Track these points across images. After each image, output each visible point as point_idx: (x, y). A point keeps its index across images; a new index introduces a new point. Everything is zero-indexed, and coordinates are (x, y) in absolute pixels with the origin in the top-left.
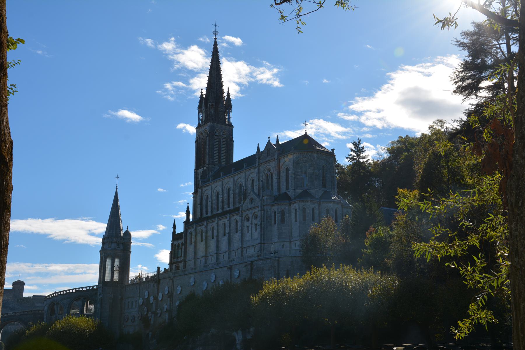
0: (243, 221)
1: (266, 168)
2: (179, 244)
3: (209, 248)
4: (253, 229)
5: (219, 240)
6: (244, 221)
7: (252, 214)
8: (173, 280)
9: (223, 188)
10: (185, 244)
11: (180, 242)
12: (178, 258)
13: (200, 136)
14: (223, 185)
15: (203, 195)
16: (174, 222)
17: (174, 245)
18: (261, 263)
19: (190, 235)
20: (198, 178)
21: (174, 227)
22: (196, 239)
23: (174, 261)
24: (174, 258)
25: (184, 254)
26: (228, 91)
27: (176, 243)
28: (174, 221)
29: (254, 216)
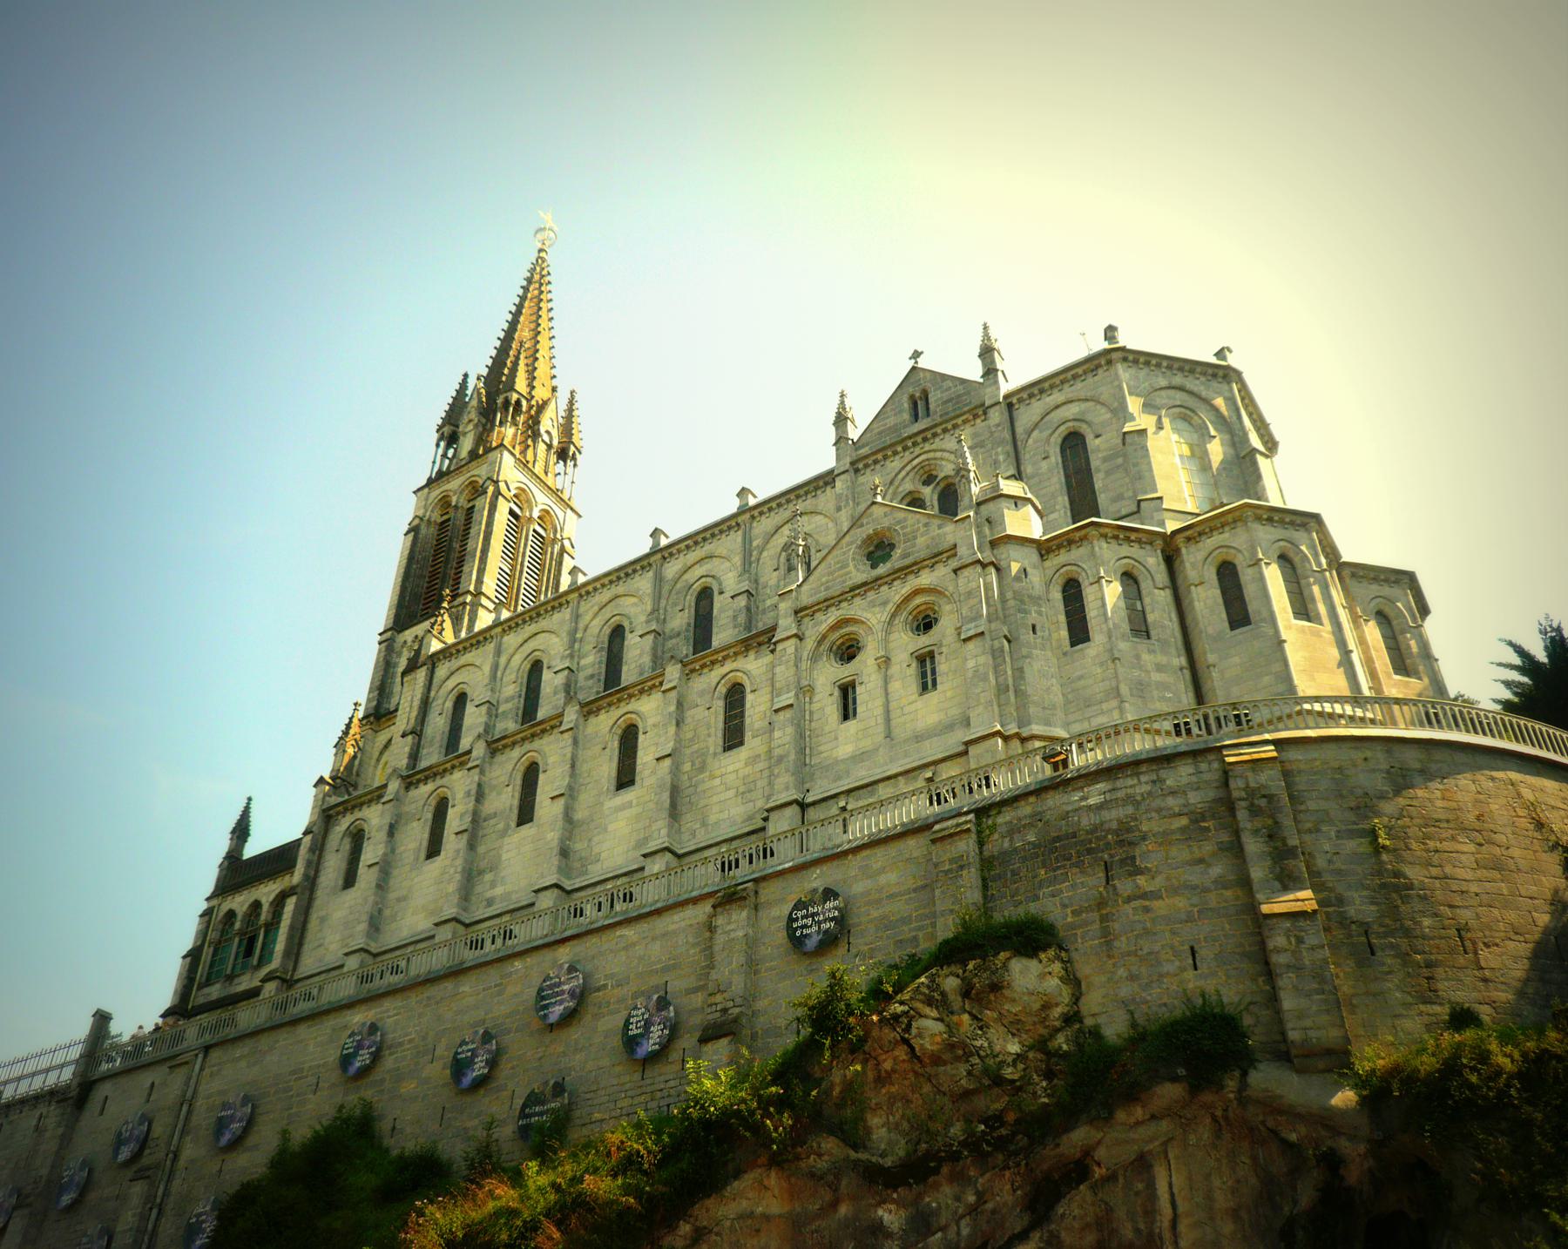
0: (804, 665)
2: (256, 905)
3: (488, 877)
4: (895, 686)
5: (579, 815)
7: (890, 607)
9: (576, 630)
11: (266, 892)
13: (432, 511)
14: (577, 617)
15: (433, 694)
17: (221, 914)
18: (1091, 801)
19: (347, 845)
20: (396, 665)
21: (241, 831)
22: (393, 851)
23: (201, 1000)
24: (208, 983)
25: (290, 938)
26: (571, 402)
27: (239, 903)
28: (248, 804)
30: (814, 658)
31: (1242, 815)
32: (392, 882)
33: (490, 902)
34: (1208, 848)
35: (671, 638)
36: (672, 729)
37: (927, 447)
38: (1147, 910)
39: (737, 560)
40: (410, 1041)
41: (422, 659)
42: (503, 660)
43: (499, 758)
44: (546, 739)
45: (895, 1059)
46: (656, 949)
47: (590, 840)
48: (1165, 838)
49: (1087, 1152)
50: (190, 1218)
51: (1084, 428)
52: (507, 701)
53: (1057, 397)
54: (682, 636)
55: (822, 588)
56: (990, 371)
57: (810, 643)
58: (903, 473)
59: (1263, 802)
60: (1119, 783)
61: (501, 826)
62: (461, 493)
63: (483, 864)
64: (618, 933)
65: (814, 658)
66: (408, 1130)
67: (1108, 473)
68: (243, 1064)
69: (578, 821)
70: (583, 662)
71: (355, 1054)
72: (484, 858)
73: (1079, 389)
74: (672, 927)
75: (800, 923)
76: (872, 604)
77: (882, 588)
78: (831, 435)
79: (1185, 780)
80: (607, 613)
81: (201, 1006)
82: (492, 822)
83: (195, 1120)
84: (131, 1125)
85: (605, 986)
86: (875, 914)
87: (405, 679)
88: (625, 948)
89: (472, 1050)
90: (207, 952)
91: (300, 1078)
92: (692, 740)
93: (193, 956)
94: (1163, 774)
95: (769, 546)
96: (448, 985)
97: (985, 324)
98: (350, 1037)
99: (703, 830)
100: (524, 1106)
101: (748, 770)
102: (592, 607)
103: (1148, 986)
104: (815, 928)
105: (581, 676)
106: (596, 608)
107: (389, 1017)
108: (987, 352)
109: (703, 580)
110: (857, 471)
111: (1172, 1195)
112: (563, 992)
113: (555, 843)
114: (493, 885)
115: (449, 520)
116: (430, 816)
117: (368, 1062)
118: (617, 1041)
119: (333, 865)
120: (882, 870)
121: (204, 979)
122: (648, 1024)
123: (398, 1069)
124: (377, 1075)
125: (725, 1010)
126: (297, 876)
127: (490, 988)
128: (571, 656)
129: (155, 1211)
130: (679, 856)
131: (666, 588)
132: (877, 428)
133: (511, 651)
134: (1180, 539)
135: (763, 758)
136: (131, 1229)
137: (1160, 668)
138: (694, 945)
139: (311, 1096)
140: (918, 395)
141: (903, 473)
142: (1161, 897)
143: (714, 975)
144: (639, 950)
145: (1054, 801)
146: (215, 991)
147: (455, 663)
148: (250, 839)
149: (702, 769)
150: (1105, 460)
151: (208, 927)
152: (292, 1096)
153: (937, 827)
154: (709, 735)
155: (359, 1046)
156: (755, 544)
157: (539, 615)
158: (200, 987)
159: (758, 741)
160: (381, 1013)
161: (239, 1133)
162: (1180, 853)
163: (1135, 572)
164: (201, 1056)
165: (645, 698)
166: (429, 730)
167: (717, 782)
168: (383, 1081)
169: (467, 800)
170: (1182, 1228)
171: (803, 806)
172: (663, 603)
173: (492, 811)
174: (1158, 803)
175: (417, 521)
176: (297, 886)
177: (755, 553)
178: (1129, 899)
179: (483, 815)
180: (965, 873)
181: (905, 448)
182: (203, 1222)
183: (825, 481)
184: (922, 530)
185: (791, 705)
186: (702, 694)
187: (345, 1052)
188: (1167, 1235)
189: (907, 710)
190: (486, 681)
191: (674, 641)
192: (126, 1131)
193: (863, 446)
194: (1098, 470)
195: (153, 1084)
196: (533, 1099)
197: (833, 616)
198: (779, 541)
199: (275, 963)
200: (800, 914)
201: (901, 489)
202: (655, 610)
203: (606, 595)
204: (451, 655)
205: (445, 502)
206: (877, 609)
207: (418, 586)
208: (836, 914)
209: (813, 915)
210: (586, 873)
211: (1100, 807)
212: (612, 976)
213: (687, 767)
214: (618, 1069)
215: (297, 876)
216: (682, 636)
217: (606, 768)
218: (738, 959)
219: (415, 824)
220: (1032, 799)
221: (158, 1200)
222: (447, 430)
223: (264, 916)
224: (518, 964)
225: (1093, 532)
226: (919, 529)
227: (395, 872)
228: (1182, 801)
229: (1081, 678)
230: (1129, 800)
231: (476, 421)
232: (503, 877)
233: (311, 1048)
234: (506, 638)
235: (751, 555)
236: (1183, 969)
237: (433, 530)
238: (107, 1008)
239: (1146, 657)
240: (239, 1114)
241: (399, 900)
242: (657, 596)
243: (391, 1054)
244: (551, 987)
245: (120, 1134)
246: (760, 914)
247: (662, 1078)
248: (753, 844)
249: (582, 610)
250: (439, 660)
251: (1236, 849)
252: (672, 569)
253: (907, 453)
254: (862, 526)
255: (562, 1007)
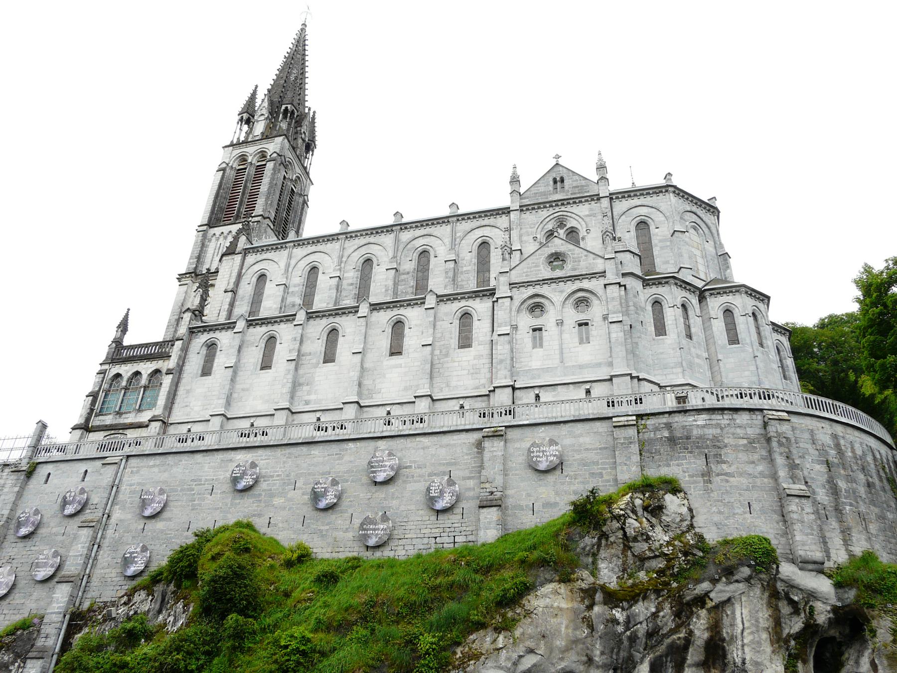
1: (552, 217)
2: (137, 373)
3: (305, 388)
4: (566, 336)
6: (519, 311)
7: (565, 294)
8: (122, 467)
10: (178, 372)
11: (146, 368)
12: (119, 413)
13: (234, 162)
15: (244, 271)
16: (127, 316)
17: (112, 375)
18: (699, 423)
19: (204, 351)
21: (123, 326)
22: (239, 361)
24: (100, 414)
25: (168, 399)
27: (126, 370)
28: (128, 312)
29: (572, 300)
30: (519, 311)
31: (774, 444)
32: (238, 379)
33: (307, 403)
34: (756, 457)
35: (404, 274)
36: (431, 331)
37: (563, 208)
38: (727, 481)
39: (447, 241)
40: (278, 476)
41: (238, 250)
42: (293, 262)
43: (312, 322)
44: (344, 317)
45: (616, 536)
46: (443, 452)
47: (374, 380)
48: (736, 448)
49: (707, 594)
50: (125, 554)
51: (649, 221)
52: (295, 286)
53: (636, 201)
54: (411, 274)
55: (524, 275)
56: (603, 179)
57: (517, 302)
58: (548, 219)
59: (784, 440)
60: (713, 417)
61: (314, 361)
62: (255, 156)
63: (302, 380)
64: (417, 439)
65: (519, 311)
66: (280, 525)
67: (662, 248)
68: (156, 470)
69: (366, 368)
70: (346, 275)
71: (241, 478)
72: (303, 377)
73: (648, 200)
74: (452, 442)
75: (535, 454)
76: (555, 290)
77: (560, 283)
78: (509, 189)
79: (745, 422)
80: (363, 251)
81: (98, 426)
82: (308, 358)
83: (121, 497)
84: (73, 494)
85: (410, 467)
86: (577, 457)
87: (224, 258)
88: (423, 448)
89: (325, 488)
90: (101, 395)
91: (199, 485)
92: (439, 338)
93: (94, 395)
94: (735, 416)
95: (466, 238)
96: (304, 449)
97: (599, 151)
98: (237, 467)
99: (447, 389)
100: (362, 524)
101: (475, 362)
102: (354, 245)
103: (727, 518)
104: (544, 459)
105: (345, 282)
106: (356, 247)
107: (261, 460)
108: (601, 167)
109: (425, 247)
110: (522, 210)
111: (742, 618)
112: (386, 466)
113: (356, 378)
114: (309, 393)
115: (245, 169)
116: (263, 346)
117: (251, 483)
118: (420, 498)
119: (195, 361)
120: (581, 435)
121: (98, 411)
122: (442, 492)
123: (271, 490)
124: (256, 491)
125: (492, 493)
126: (172, 363)
127: (333, 455)
128: (340, 270)
129: (96, 546)
130: (433, 400)
131: (401, 247)
132: (534, 190)
133: (299, 258)
134: (707, 294)
135: (484, 357)
136: (81, 555)
137: (698, 356)
138: (467, 454)
139: (209, 496)
140: (558, 179)
141: (548, 219)
142: (734, 477)
143: (484, 472)
144: (432, 450)
145: (678, 419)
146: (108, 420)
147: (259, 257)
148: (127, 333)
149: (447, 355)
150: (660, 241)
151: (103, 381)
152: (194, 494)
153: (614, 419)
154: (451, 338)
155: (244, 473)
156: (458, 235)
157: (318, 242)
158: (96, 416)
159: (481, 347)
160: (256, 456)
161: (159, 510)
162: (743, 456)
163: (687, 305)
164: (124, 461)
165: (409, 308)
166: (241, 292)
167: (456, 364)
168: (260, 495)
169: (295, 342)
170: (745, 634)
171: (514, 389)
172: (399, 254)
173: (308, 351)
174: (732, 430)
175: (224, 165)
176: (173, 369)
177: (458, 240)
178: (718, 475)
179: (302, 352)
180: (632, 446)
181: (551, 206)
182: (135, 557)
183: (506, 211)
184: (584, 258)
185: (508, 334)
186: (446, 314)
187: (234, 475)
188: (739, 636)
189: (572, 350)
190: (283, 271)
191: (405, 276)
192: (70, 496)
193: (525, 198)
194: (656, 245)
195: (86, 471)
196: (367, 521)
197: (531, 291)
198: (472, 237)
199: (158, 411)
200: (535, 449)
201: (546, 227)
202: (394, 257)
203: (363, 241)
204: (258, 251)
205: (243, 159)
206: (557, 294)
207: (222, 203)
208: (557, 453)
209: (543, 451)
210: (372, 398)
211: (704, 426)
212: (415, 462)
213: (437, 352)
214: (421, 512)
215: (172, 363)
216: (411, 274)
217: (384, 342)
218: (499, 467)
219: (254, 348)
220: (667, 415)
221: (98, 540)
222: (245, 116)
223: (144, 380)
224: (351, 445)
225: (672, 281)
226: (582, 257)
227: (240, 373)
228: (744, 432)
229: (662, 353)
230: (718, 426)
231: (266, 116)
232: (316, 390)
233: (206, 469)
234: (295, 250)
235: (455, 240)
236: (745, 513)
237: (233, 173)
238: (45, 420)
239: (693, 350)
240: (157, 499)
241: (243, 390)
242: (396, 250)
243: (265, 481)
244: (377, 462)
245: (65, 498)
246: (508, 444)
247: (449, 521)
248: (480, 404)
249: (346, 246)
250: (249, 252)
251: (772, 461)
252: (406, 236)
253: (551, 209)
254: (548, 247)
255: (385, 474)
